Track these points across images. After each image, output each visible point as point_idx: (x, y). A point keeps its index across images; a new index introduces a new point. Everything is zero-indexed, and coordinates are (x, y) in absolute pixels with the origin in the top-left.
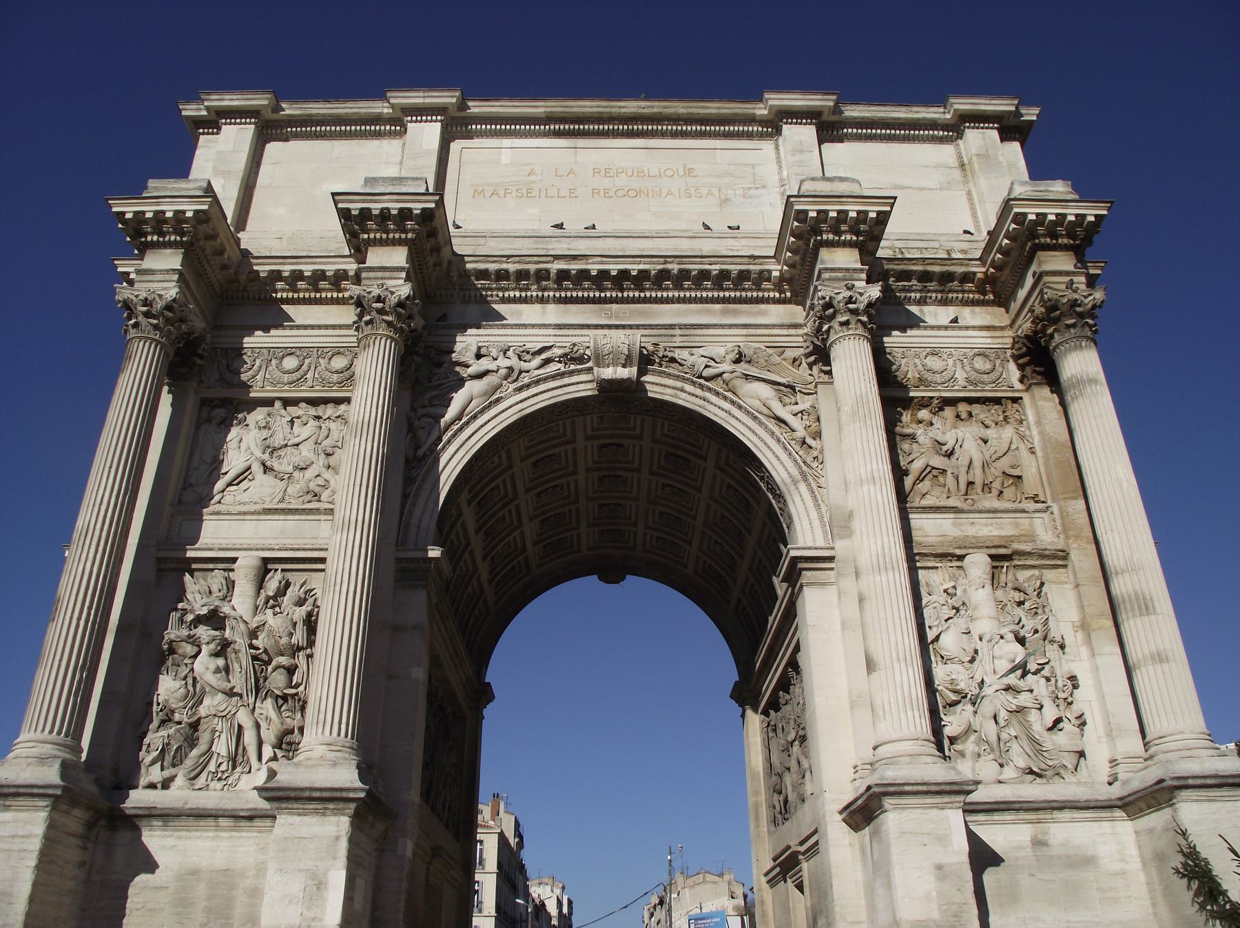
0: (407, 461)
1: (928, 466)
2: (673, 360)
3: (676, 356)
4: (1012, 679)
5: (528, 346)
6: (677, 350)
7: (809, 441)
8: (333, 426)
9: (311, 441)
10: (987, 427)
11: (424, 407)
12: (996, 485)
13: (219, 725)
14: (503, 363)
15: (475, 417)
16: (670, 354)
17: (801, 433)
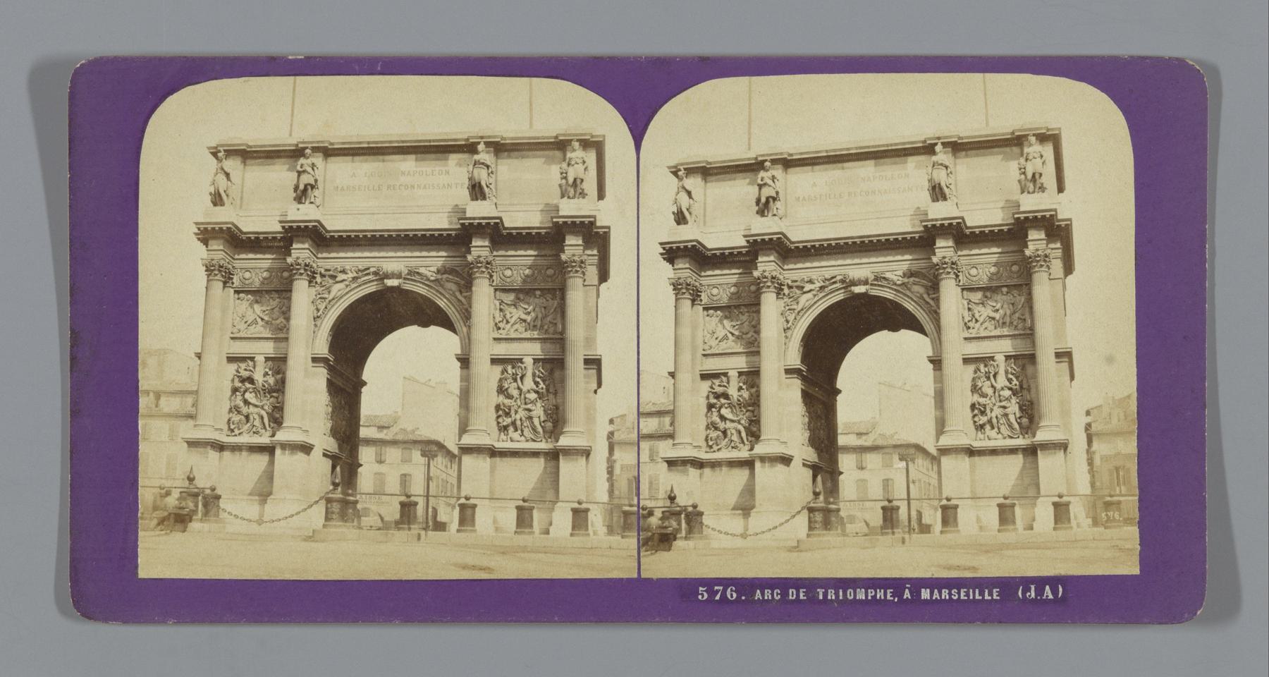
0: (314, 318)
1: (519, 318)
2: (418, 273)
3: (420, 271)
4: (529, 406)
5: (360, 267)
6: (421, 268)
7: (469, 309)
8: (285, 301)
9: (277, 309)
10: (547, 301)
11: (319, 294)
12: (546, 327)
13: (256, 417)
14: (351, 275)
15: (339, 299)
16: (417, 271)
17: (466, 306)
